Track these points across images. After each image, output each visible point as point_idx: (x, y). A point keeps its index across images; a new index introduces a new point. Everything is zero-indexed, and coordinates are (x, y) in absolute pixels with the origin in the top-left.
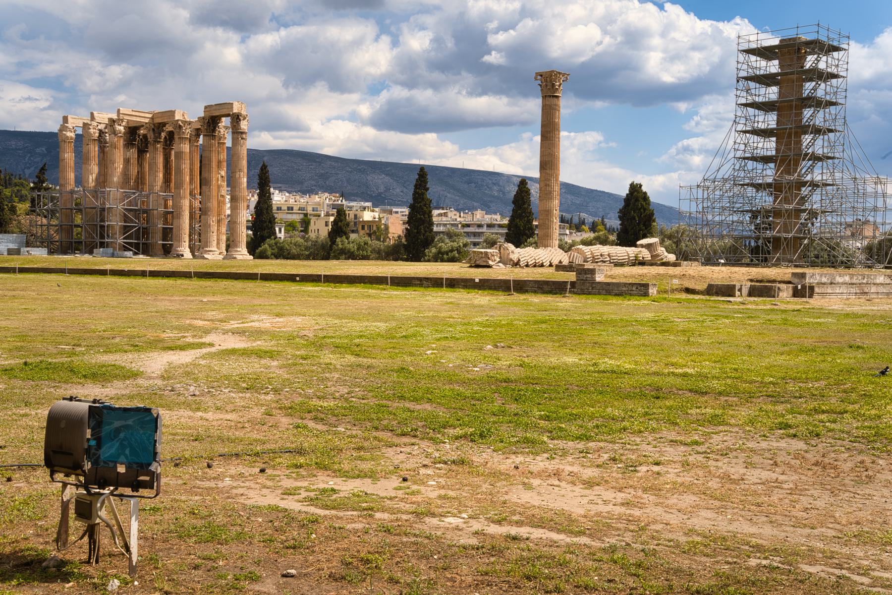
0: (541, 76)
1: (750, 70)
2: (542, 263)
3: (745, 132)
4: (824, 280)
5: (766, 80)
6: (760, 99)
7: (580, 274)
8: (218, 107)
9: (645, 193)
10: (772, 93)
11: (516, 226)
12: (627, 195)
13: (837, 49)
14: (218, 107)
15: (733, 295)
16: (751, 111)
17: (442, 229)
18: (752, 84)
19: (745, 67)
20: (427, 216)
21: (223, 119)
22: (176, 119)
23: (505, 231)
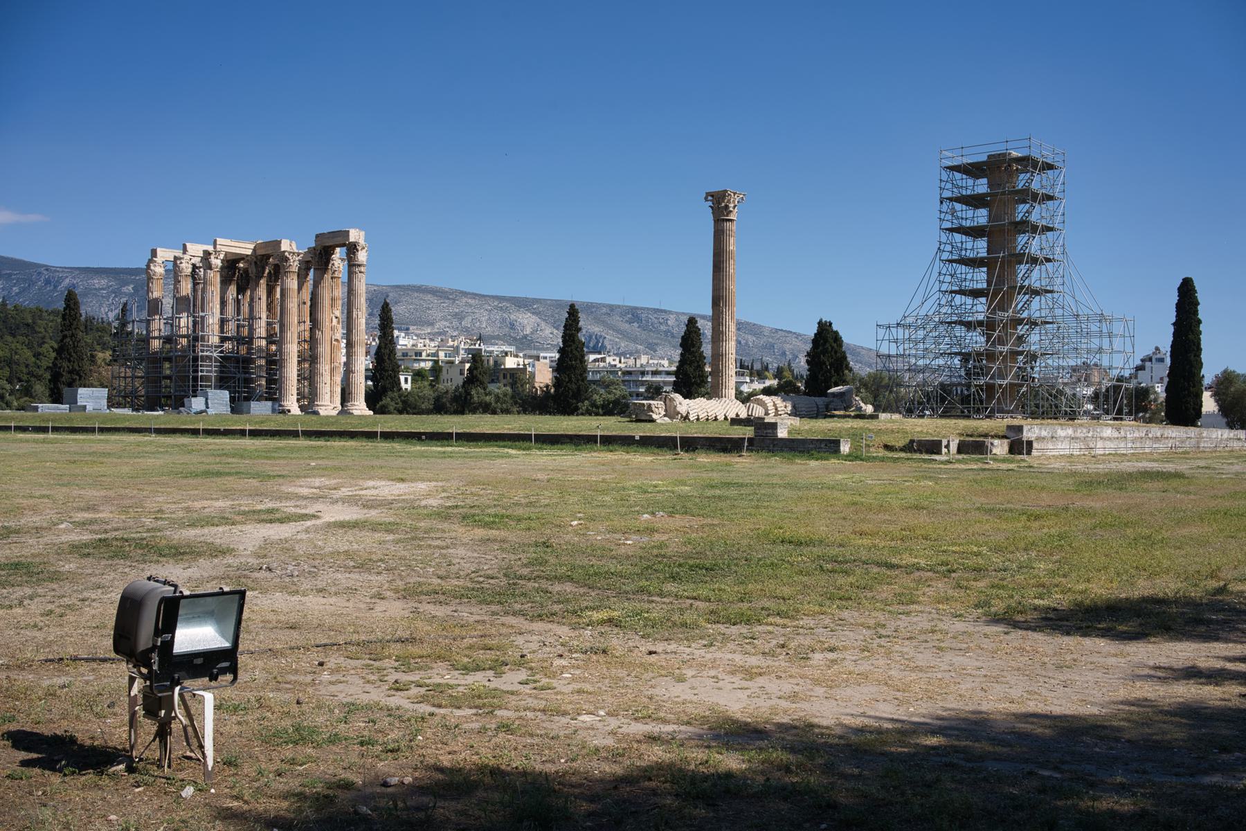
0: (712, 196)
2: (716, 417)
3: (951, 261)
5: (974, 201)
6: (968, 224)
7: (759, 429)
9: (836, 333)
10: (981, 217)
11: (686, 374)
12: (815, 335)
15: (939, 452)
16: (958, 237)
17: (598, 377)
18: (958, 206)
19: (949, 186)
20: (578, 362)
21: (338, 250)
22: (283, 249)
23: (673, 379)
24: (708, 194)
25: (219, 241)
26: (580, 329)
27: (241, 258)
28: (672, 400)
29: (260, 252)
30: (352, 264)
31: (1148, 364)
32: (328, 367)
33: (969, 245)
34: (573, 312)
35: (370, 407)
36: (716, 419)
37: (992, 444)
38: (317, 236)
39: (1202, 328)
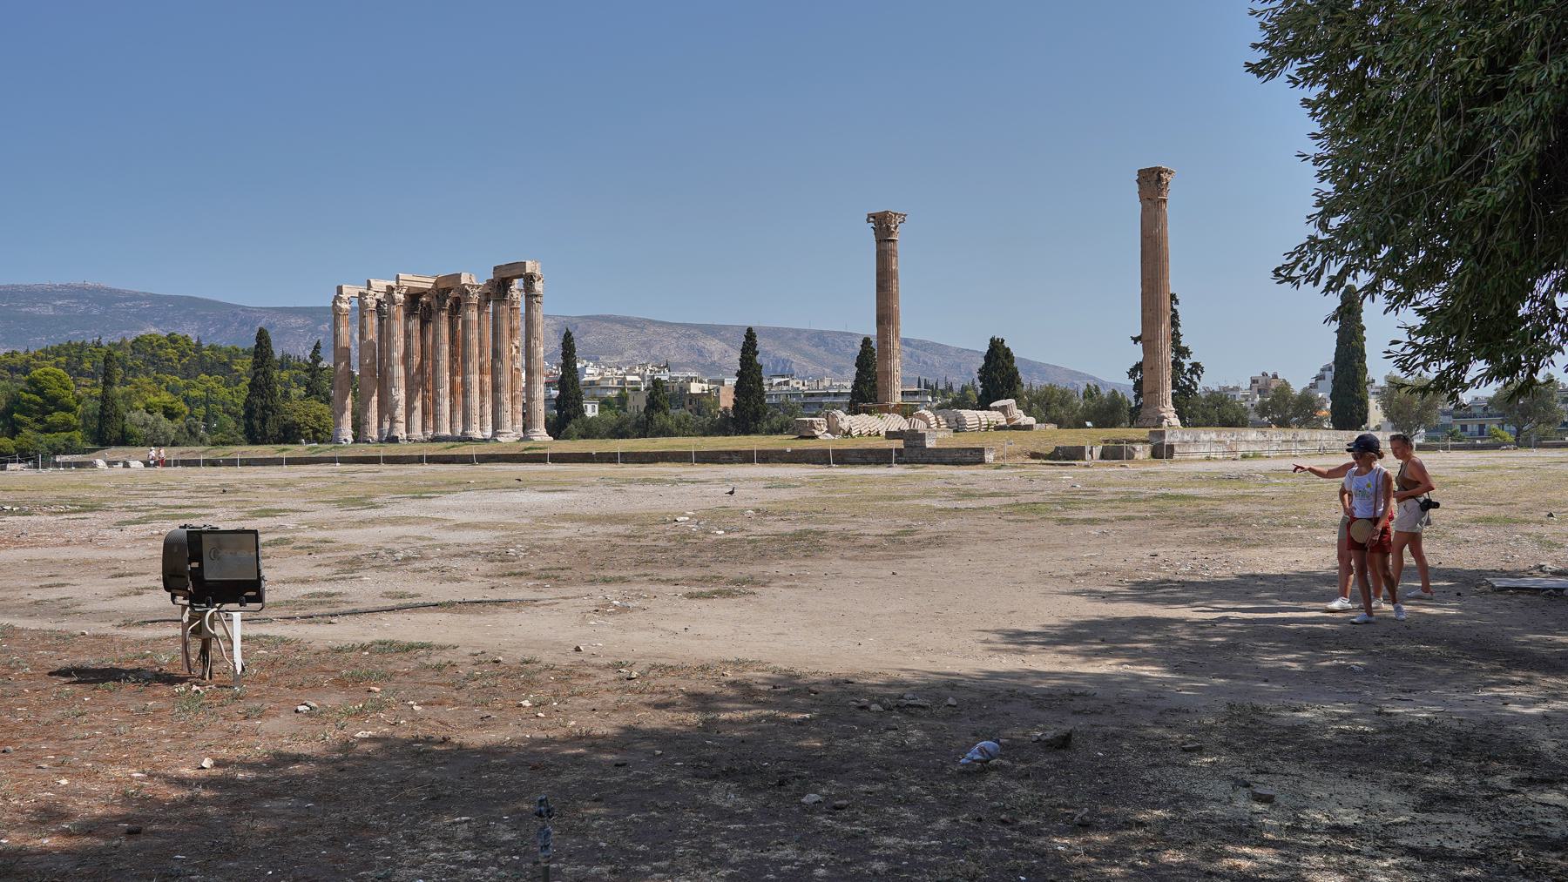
0: (874, 217)
4: (1186, 438)
9: (1008, 349)
15: (1083, 459)
21: (516, 281)
24: (870, 216)
25: (402, 276)
26: (758, 353)
27: (423, 292)
28: (834, 416)
29: (442, 286)
30: (530, 294)
32: (508, 396)
34: (750, 335)
35: (550, 433)
36: (878, 434)
37: (1134, 449)
38: (495, 268)
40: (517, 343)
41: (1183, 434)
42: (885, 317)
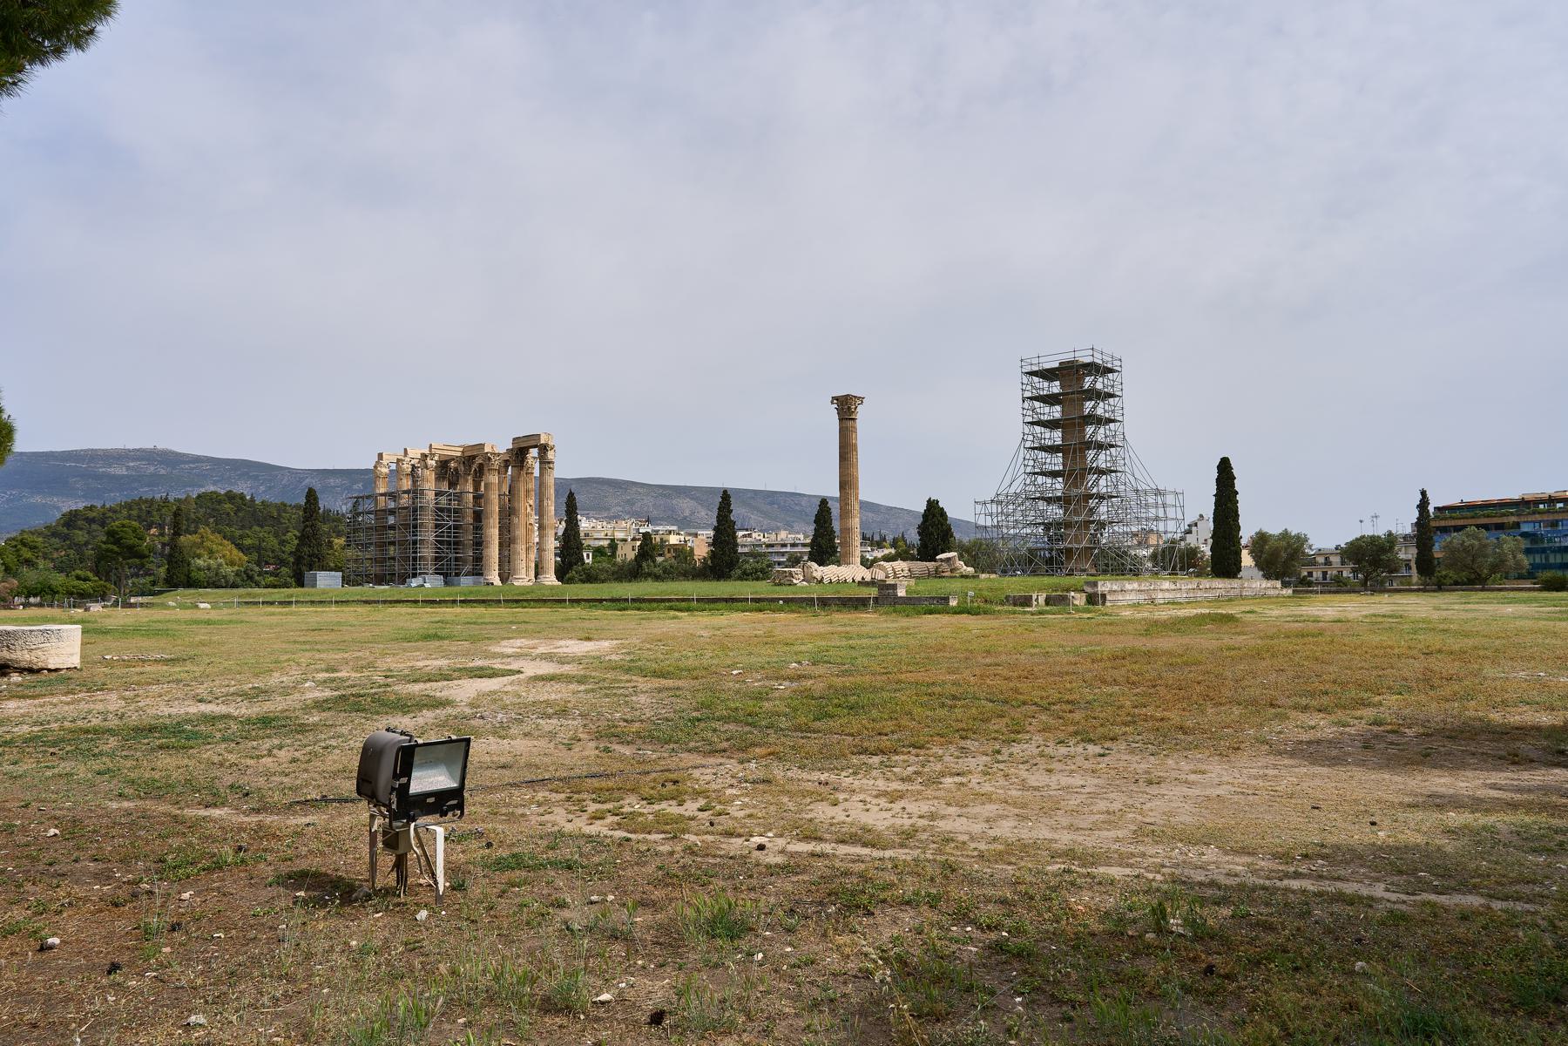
0: (837, 400)
1: (1034, 391)
2: (846, 580)
4: (1115, 588)
5: (1050, 400)
6: (1046, 418)
8: (525, 439)
10: (1056, 412)
11: (820, 546)
13: (1111, 371)
14: (525, 439)
16: (1038, 429)
17: (746, 550)
18: (1037, 404)
21: (531, 450)
23: (808, 549)
29: (466, 454)
31: (1194, 529)
32: (524, 547)
33: (1047, 436)
34: (726, 496)
38: (514, 439)
39: (1238, 497)
40: (531, 502)
41: (1112, 584)
42: (847, 482)
